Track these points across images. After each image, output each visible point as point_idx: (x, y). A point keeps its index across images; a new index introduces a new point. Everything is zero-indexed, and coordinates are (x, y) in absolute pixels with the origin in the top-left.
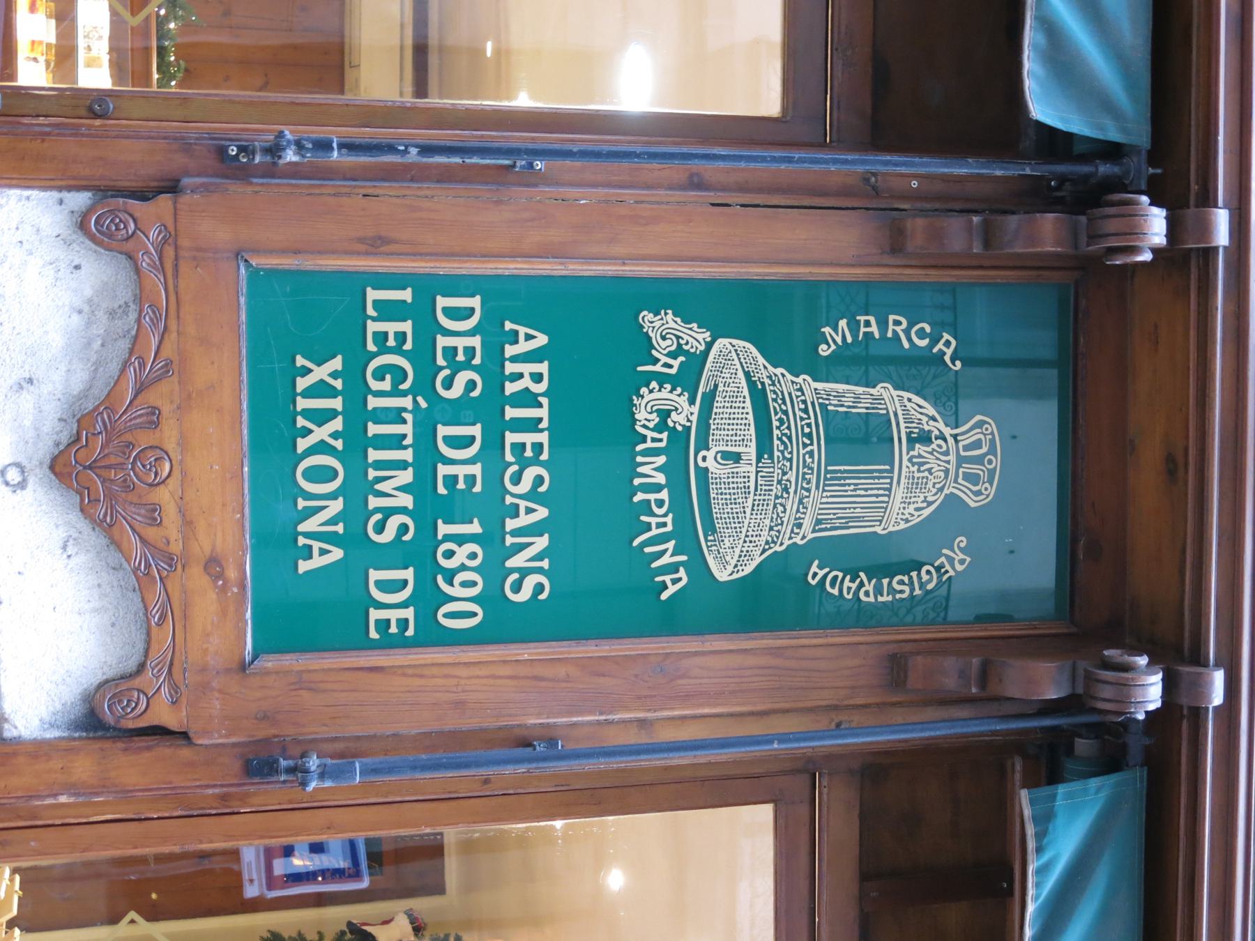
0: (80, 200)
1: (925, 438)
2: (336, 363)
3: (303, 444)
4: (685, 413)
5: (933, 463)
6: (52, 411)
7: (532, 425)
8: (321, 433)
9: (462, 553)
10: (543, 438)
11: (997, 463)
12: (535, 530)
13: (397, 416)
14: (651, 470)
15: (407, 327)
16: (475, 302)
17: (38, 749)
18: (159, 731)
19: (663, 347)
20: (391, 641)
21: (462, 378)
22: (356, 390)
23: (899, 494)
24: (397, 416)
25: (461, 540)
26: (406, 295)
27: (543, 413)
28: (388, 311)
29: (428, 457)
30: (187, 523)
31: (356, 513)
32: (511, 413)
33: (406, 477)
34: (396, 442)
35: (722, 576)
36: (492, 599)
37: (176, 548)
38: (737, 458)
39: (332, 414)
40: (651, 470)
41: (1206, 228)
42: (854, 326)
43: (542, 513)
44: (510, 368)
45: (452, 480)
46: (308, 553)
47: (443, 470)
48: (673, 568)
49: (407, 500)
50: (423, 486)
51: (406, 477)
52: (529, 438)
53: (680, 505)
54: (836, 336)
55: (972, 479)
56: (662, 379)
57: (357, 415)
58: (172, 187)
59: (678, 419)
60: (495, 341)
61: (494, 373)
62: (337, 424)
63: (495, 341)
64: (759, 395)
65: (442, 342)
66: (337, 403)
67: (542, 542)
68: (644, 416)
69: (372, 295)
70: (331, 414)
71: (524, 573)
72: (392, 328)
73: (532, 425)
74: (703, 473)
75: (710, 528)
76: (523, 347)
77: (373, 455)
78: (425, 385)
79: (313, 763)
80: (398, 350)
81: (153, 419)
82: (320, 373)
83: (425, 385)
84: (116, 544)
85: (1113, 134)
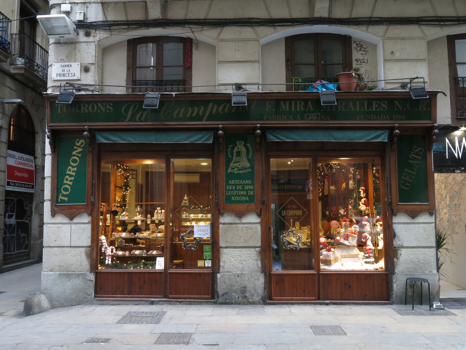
0: (220, 216)
1: (238, 148)
2: (232, 197)
3: (238, 200)
4: (236, 169)
5: (240, 147)
6: (236, 218)
7: (237, 182)
8: (238, 198)
9: (247, 187)
10: (238, 181)
11: (240, 141)
12: (245, 182)
13: (236, 192)
14: (241, 172)
15: (229, 192)
16: (227, 186)
17: (262, 220)
18: (260, 211)
19: (231, 171)
20: (254, 193)
21: (233, 187)
22: (234, 196)
23: (243, 150)
24: (236, 192)
25: (246, 187)
26: (227, 192)
27: (236, 181)
28: (228, 193)
29: (239, 190)
30: (244, 209)
31: (244, 196)
32: (236, 183)
33: (241, 192)
34: (238, 192)
35: (249, 166)
36: (251, 185)
37: (246, 209)
38: (240, 165)
39: (236, 198)
40: (241, 172)
41: (220, 127)
42: (229, 154)
43: (244, 181)
44: (233, 183)
45: (241, 188)
46: (247, 199)
48: (249, 170)
49: (243, 192)
50: (242, 190)
51: (241, 192)
52: (238, 182)
53: (244, 169)
54: (230, 156)
55: (242, 143)
56: (233, 171)
57: (236, 195)
58: (219, 209)
59: (237, 170)
60: (230, 185)
61: (233, 185)
62: (237, 197)
63: (230, 185)
64: (235, 163)
65: (230, 189)
66: (235, 197)
67: (246, 181)
68: (236, 172)
70: (236, 198)
71: (249, 182)
72: (229, 193)
74: (241, 167)
75: (246, 167)
76: (231, 182)
77: (239, 194)
78: (234, 190)
79: (263, 199)
80: (231, 192)
81: (236, 211)
82: (233, 198)
83: (234, 190)
84: (246, 214)
85: (213, 135)
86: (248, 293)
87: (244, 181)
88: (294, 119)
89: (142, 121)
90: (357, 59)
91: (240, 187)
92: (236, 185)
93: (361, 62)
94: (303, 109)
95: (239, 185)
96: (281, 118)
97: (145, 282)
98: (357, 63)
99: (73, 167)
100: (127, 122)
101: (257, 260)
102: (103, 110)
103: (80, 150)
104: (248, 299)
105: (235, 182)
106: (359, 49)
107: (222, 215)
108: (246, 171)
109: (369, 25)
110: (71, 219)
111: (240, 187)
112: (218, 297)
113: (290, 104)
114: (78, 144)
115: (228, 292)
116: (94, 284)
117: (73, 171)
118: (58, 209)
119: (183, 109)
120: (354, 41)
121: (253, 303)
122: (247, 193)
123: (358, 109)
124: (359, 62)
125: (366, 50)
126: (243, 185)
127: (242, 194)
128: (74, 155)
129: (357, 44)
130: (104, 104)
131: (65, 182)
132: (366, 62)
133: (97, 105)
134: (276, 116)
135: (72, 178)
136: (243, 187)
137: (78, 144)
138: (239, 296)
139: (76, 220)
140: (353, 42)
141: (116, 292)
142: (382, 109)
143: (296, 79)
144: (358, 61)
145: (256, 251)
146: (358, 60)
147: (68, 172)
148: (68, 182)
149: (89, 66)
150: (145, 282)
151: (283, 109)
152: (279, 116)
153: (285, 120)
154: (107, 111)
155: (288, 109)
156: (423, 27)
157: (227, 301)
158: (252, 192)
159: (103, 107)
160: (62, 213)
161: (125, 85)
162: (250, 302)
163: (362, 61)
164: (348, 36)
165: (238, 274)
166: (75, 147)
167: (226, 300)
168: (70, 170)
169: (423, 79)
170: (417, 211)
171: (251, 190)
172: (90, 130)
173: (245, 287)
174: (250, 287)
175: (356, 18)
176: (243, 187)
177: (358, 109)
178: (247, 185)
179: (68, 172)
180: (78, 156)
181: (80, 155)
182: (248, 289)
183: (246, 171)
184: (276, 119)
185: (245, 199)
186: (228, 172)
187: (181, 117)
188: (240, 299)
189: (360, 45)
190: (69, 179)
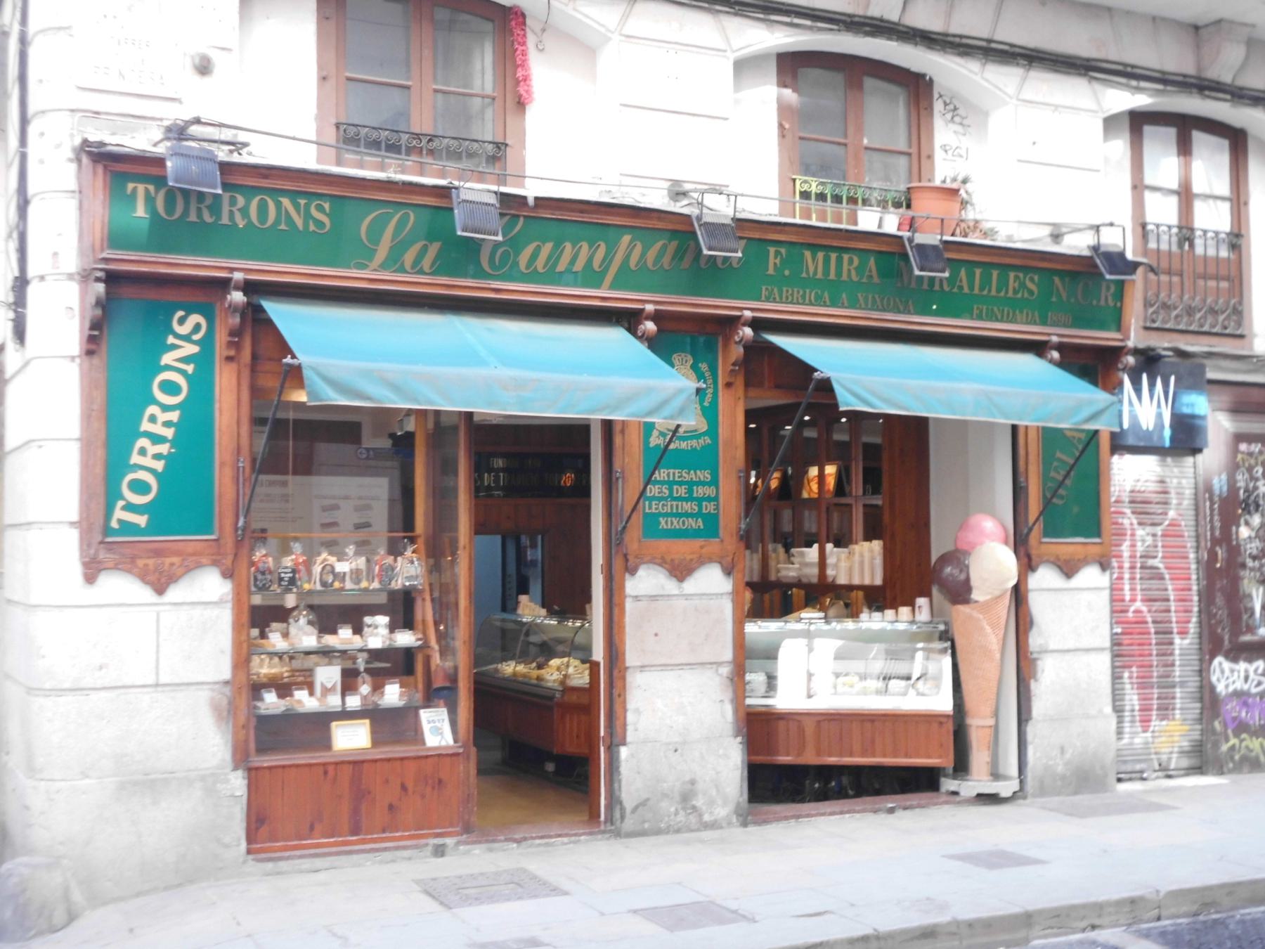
2: (661, 519)
7: (674, 474)
9: (700, 491)
10: (677, 471)
12: (696, 473)
13: (672, 506)
19: (658, 442)
20: (717, 508)
22: (666, 515)
24: (672, 506)
25: (697, 492)
32: (671, 479)
34: (677, 506)
35: (706, 428)
36: (709, 484)
39: (672, 521)
43: (692, 472)
44: (662, 479)
47: (683, 495)
48: (704, 441)
50: (686, 500)
52: (677, 475)
55: (686, 362)
58: (625, 556)
62: (674, 519)
67: (698, 472)
69: (647, 511)
70: (672, 521)
71: (704, 476)
72: (654, 507)
73: (674, 474)
75: (696, 431)
78: (665, 499)
80: (658, 505)
83: (665, 499)
86: (700, 796)
87: (692, 472)
88: (834, 304)
89: (421, 272)
90: (945, 146)
91: (682, 491)
92: (671, 484)
93: (953, 155)
94: (855, 278)
95: (680, 483)
96: (803, 297)
97: (404, 788)
98: (943, 153)
99: (166, 408)
100: (375, 270)
101: (721, 701)
102: (299, 222)
103: (191, 349)
104: (701, 816)
105: (668, 475)
106: (949, 116)
107: (633, 571)
108: (698, 443)
109: (987, 60)
110: (160, 591)
111: (682, 491)
112: (623, 817)
113: (827, 260)
114: (184, 330)
115: (648, 800)
116: (245, 807)
117: (167, 424)
118: (112, 556)
119: (548, 247)
120: (939, 93)
121: (713, 826)
122: (700, 507)
123: (976, 291)
124: (950, 152)
125: (965, 122)
126: (691, 484)
127: (686, 512)
128: (168, 368)
129: (946, 104)
130: (302, 202)
131: (135, 459)
132: (965, 155)
133: (279, 205)
134: (790, 292)
135: (164, 449)
136: (690, 491)
137: (184, 330)
138: (676, 810)
139: (175, 593)
140: (936, 96)
141: (312, 828)
142: (1026, 295)
143: (805, 182)
144: (946, 151)
145: (721, 675)
146: (948, 148)
147: (146, 426)
148: (148, 461)
149: (216, 56)
150: (404, 788)
151: (808, 272)
152: (798, 292)
153: (811, 304)
154: (312, 227)
155: (819, 275)
156: (1097, 86)
157: (646, 825)
158: (712, 503)
159: (298, 212)
160: (129, 571)
161: (314, 138)
162: (706, 822)
163: (955, 153)
164: (928, 78)
165: (676, 743)
166: (171, 340)
167: (644, 822)
168: (153, 419)
169: (1121, 229)
170: (1079, 560)
171: (709, 499)
172: (250, 288)
173: (693, 782)
174: (705, 781)
175: (961, 37)
176: (690, 491)
177: (976, 291)
178: (701, 483)
179: (146, 426)
180: (183, 372)
181: (190, 368)
182: (700, 786)
183: (698, 443)
184: (790, 300)
185: (694, 525)
186: (651, 445)
187: (540, 269)
188: (681, 817)
189: (951, 107)
190: (153, 450)
